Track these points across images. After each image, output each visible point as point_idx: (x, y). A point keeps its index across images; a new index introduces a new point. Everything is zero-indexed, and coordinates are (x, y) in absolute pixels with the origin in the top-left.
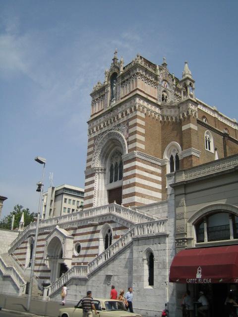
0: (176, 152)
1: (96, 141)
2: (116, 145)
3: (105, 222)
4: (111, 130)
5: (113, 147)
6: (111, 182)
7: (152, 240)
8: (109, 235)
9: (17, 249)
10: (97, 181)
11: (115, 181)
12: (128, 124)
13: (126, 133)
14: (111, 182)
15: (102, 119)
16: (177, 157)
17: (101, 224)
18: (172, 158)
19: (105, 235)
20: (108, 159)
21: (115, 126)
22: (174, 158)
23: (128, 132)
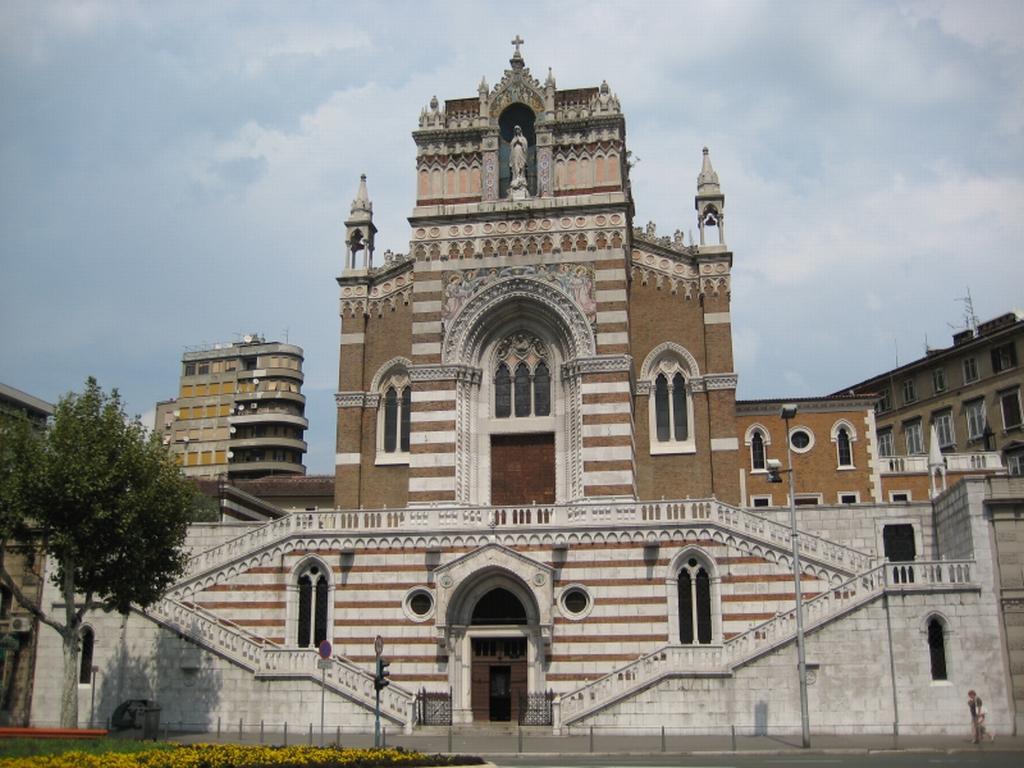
0: (676, 367)
1: (452, 286)
2: (521, 317)
3: (685, 542)
4: (522, 271)
5: (512, 320)
6: (502, 412)
7: (941, 596)
8: (693, 572)
9: (215, 588)
10: (462, 405)
11: (523, 412)
12: (590, 276)
13: (584, 297)
14: (502, 412)
15: (479, 229)
16: (679, 378)
17: (672, 543)
18: (661, 379)
19: (679, 572)
20: (490, 348)
21: (538, 267)
22: (670, 383)
23: (590, 294)
